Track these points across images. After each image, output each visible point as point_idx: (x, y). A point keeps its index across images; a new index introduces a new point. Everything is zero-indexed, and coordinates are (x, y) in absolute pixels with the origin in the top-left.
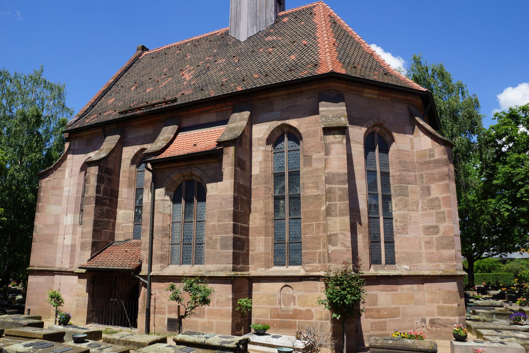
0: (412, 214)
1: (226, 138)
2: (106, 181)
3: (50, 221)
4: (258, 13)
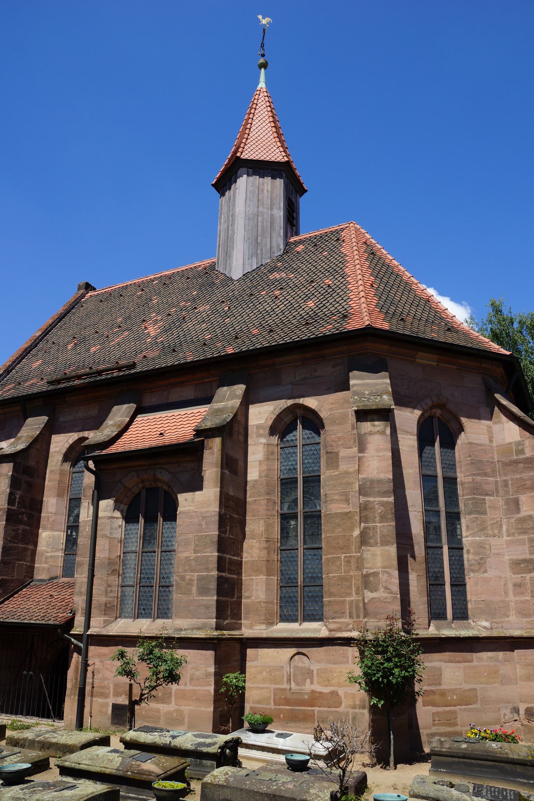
0: (493, 541)
1: (209, 424)
4: (259, 238)
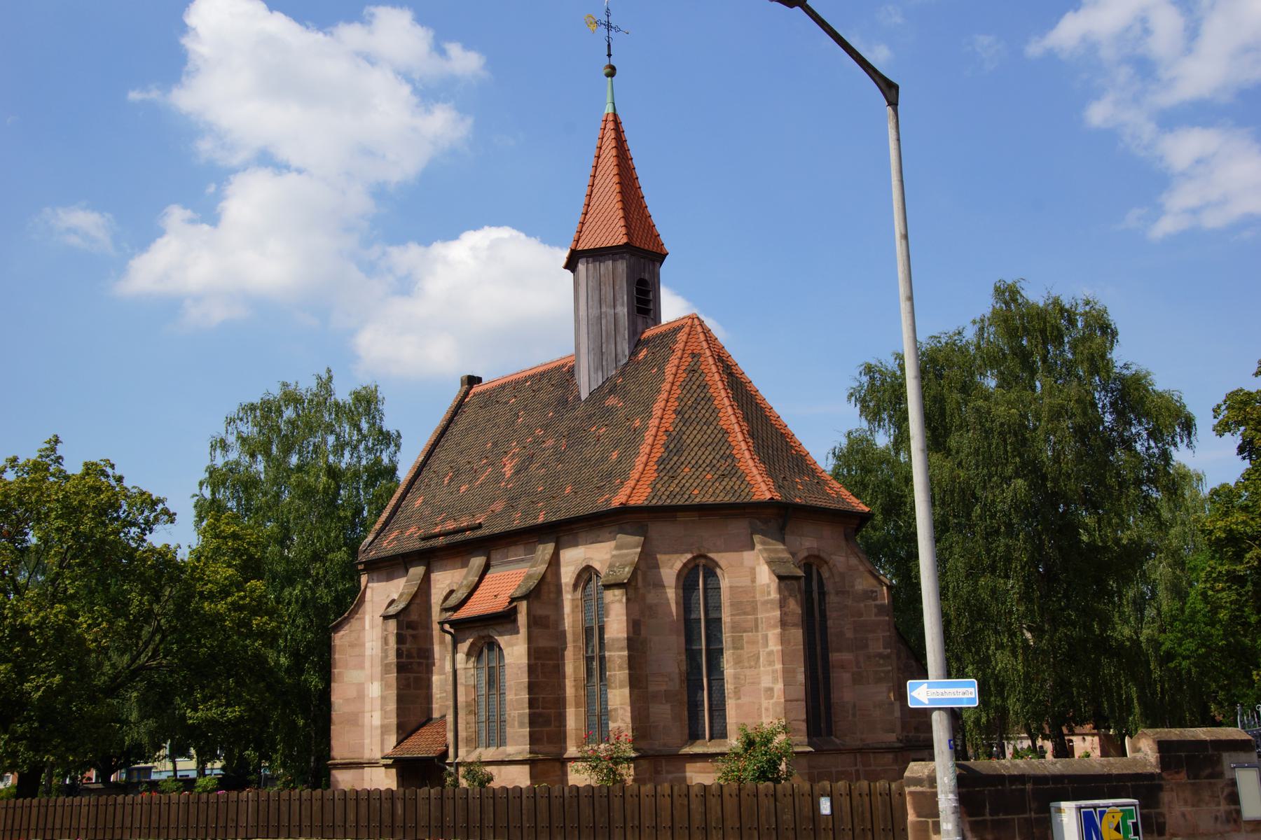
0: (748, 672)
1: (518, 594)
2: (409, 639)
3: (352, 693)
